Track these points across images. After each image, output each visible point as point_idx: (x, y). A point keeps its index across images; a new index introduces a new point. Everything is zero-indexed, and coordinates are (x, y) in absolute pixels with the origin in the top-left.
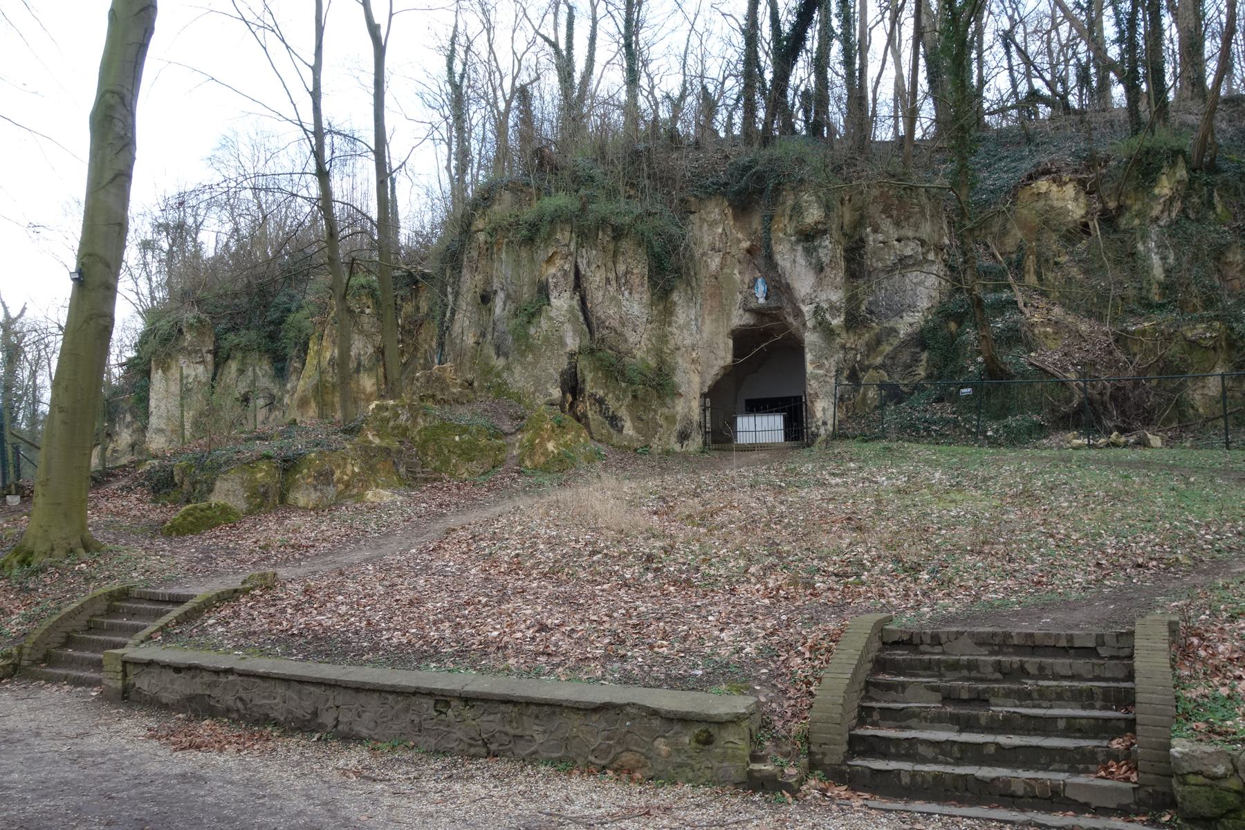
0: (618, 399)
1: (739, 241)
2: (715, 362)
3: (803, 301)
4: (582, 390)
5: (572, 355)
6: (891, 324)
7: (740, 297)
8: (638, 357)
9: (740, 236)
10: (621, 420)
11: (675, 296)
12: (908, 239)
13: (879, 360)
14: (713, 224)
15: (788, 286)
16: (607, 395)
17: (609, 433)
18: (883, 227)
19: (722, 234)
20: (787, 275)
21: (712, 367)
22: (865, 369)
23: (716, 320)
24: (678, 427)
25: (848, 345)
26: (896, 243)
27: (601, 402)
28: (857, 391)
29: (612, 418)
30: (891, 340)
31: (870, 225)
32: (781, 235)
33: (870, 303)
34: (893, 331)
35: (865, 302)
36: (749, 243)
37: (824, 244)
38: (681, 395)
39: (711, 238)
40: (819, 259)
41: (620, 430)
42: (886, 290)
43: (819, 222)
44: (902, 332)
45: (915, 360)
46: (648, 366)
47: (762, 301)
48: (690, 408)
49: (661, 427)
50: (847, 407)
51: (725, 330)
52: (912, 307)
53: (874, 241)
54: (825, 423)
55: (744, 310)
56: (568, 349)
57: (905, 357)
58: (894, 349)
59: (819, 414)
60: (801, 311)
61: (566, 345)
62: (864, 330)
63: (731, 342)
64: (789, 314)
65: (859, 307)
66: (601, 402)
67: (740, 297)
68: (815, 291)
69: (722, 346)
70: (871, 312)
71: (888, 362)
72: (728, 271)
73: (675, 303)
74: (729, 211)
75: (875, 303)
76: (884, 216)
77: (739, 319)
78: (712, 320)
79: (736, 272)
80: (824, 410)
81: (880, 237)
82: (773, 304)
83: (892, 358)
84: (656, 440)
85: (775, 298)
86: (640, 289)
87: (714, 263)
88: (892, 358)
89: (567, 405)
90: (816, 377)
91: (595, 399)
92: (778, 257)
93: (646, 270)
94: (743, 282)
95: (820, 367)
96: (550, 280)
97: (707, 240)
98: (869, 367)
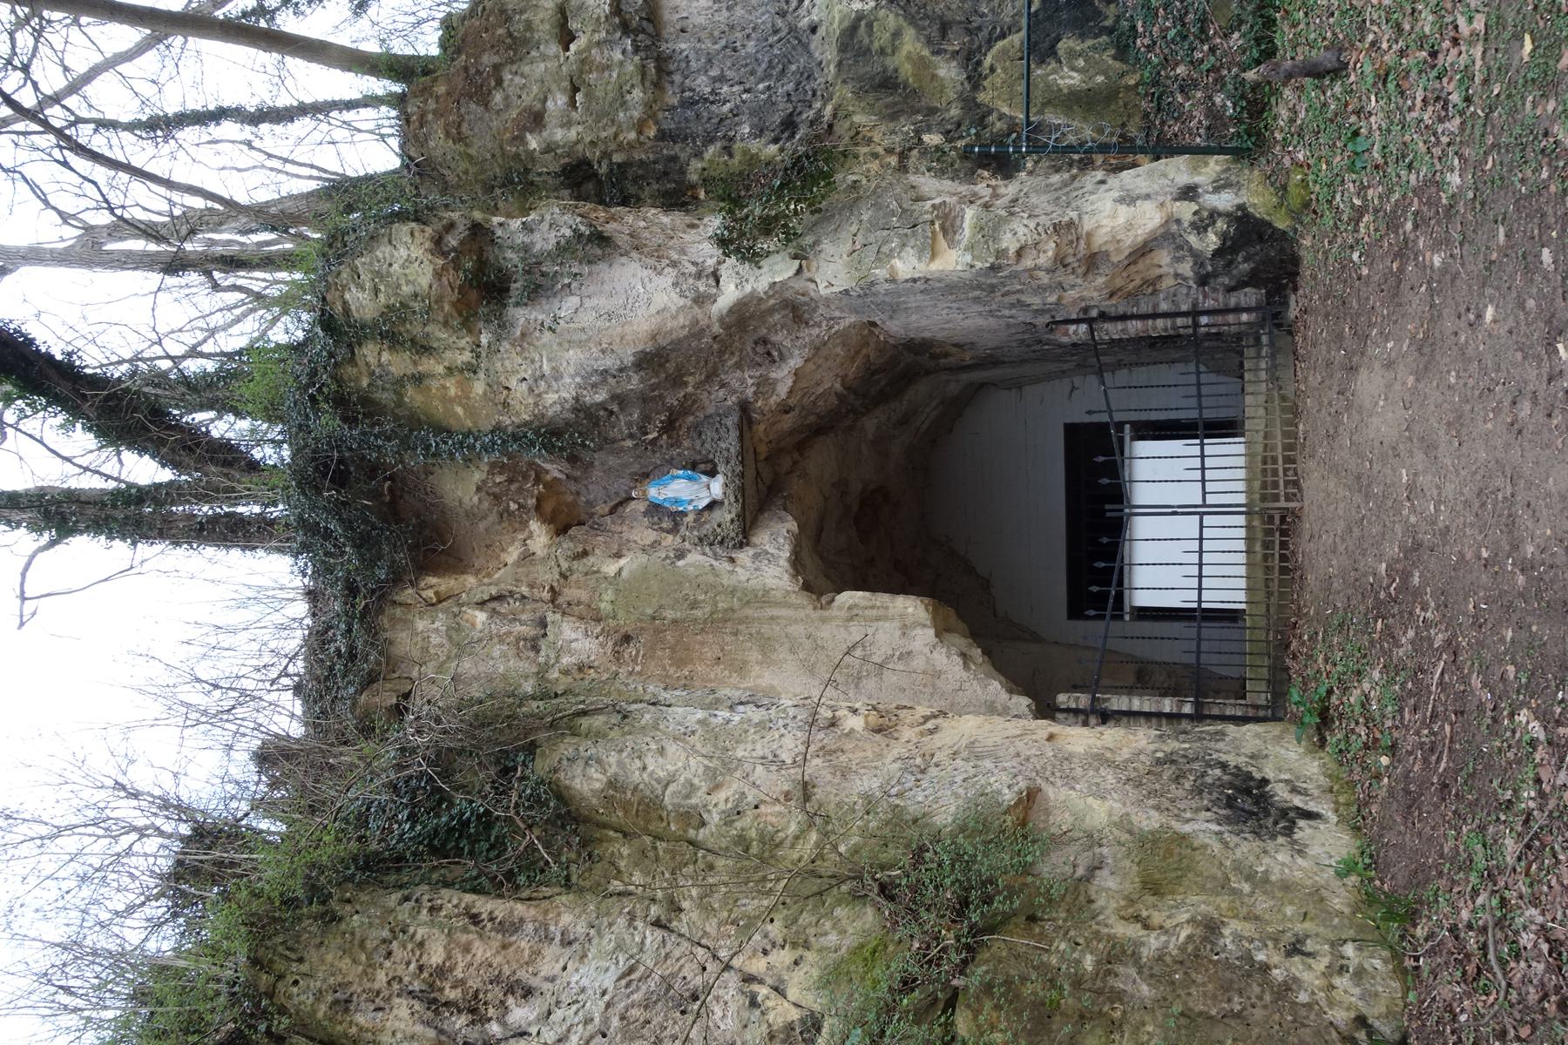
1: (527, 556)
2: (918, 663)
3: (700, 300)
8: (815, 1002)
9: (513, 554)
11: (586, 783)
13: (949, 72)
14: (461, 644)
15: (650, 360)
18: (527, 99)
20: (609, 362)
21: (938, 674)
22: (979, 115)
23: (766, 646)
24: (1203, 827)
26: (573, 47)
31: (520, 139)
32: (479, 387)
33: (759, 132)
35: (755, 145)
36: (534, 525)
37: (520, 238)
38: (1031, 797)
39: (497, 651)
40: (563, 250)
42: (721, 79)
43: (438, 241)
46: (869, 954)
47: (717, 487)
48: (1100, 760)
49: (1211, 928)
53: (567, 124)
54: (1188, 193)
55: (741, 546)
58: (912, 21)
60: (743, 317)
62: (842, 128)
63: (847, 598)
64: (765, 384)
67: (695, 557)
68: (674, 264)
70: (789, 125)
72: (609, 595)
73: (612, 784)
74: (435, 584)
75: (758, 112)
76: (498, 97)
78: (767, 661)
79: (610, 568)
80: (1129, 199)
81: (557, 102)
82: (731, 442)
83: (945, 28)
84: (1309, 974)
85: (709, 434)
88: (945, 28)
90: (988, 232)
92: (556, 399)
93: (451, 900)
95: (948, 224)
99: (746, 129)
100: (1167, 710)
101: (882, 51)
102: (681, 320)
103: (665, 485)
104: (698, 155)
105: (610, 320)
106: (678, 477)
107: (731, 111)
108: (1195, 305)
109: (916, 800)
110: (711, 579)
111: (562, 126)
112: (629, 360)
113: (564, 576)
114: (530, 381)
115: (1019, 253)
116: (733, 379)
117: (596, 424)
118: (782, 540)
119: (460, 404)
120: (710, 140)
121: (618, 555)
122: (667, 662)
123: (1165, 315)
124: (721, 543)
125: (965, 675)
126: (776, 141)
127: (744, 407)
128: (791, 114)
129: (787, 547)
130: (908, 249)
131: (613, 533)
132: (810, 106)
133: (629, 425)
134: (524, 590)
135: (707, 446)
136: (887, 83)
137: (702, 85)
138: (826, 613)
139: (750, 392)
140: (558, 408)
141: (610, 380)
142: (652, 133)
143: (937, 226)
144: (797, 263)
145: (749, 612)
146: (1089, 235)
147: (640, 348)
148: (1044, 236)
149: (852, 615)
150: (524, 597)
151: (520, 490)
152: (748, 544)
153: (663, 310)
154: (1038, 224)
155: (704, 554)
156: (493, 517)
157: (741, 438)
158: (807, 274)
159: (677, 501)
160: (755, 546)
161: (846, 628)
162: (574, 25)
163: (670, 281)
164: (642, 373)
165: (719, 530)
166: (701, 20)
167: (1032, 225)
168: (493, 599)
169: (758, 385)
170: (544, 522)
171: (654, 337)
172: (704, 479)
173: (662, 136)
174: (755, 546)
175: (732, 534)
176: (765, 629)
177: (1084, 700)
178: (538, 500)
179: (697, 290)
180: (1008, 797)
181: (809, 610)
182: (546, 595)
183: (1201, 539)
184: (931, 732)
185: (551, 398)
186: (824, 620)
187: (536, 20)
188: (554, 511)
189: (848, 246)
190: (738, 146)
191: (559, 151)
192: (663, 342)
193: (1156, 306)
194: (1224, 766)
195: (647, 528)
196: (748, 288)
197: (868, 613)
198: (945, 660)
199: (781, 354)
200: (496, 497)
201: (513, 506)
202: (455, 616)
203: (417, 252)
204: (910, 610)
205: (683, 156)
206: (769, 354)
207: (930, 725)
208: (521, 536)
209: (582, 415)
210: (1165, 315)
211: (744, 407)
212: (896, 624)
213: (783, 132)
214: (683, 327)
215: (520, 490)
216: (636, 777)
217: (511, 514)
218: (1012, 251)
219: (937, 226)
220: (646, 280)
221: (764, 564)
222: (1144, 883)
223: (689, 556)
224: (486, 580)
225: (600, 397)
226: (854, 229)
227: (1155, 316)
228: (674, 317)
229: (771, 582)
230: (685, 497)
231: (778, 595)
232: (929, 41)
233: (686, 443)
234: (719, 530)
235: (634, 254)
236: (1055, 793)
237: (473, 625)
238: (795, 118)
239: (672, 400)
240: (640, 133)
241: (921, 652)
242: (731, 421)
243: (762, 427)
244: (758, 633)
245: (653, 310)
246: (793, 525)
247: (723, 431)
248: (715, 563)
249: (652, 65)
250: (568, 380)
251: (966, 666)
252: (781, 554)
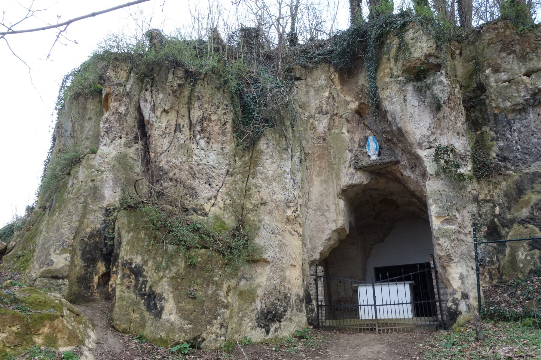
0: (158, 268)
1: (347, 103)
2: (326, 226)
3: (420, 145)
5: (108, 212)
7: (350, 155)
8: (210, 215)
9: (348, 98)
10: (162, 298)
11: (262, 145)
13: (525, 212)
14: (318, 90)
16: (145, 262)
17: (143, 318)
18: (504, 65)
19: (329, 98)
20: (398, 119)
21: (323, 232)
22: (509, 224)
23: (326, 181)
24: (259, 305)
25: (481, 197)
26: (525, 77)
27: (137, 272)
28: (502, 252)
29: (149, 295)
31: (489, 66)
32: (387, 80)
35: (495, 149)
36: (357, 103)
38: (266, 262)
39: (317, 102)
40: (434, 97)
41: (158, 314)
42: (520, 132)
43: (430, 55)
46: (223, 225)
47: (374, 157)
49: (226, 307)
50: (490, 274)
51: (335, 189)
53: (496, 82)
54: (465, 296)
55: (355, 168)
56: (105, 204)
59: (456, 284)
60: (418, 158)
61: (103, 197)
62: (500, 178)
63: (342, 203)
64: (405, 167)
66: (137, 272)
67: (350, 155)
68: (433, 133)
69: (332, 207)
70: (504, 159)
72: (337, 131)
73: (262, 152)
74: (336, 77)
75: (508, 148)
76: (504, 55)
78: (322, 182)
79: (344, 130)
80: (462, 277)
81: (504, 76)
82: (387, 159)
84: (215, 328)
86: (221, 138)
87: (322, 124)
89: (96, 279)
90: (446, 234)
91: (130, 269)
92: (387, 105)
93: (230, 117)
94: (352, 139)
95: (450, 220)
97: (314, 104)
99: (501, 144)
100: (319, 297)
101: (533, 188)
102: (413, 140)
103: (373, 141)
104: (491, 129)
105: (410, 117)
106: (376, 144)
107: (508, 138)
108: (443, 301)
109: (263, 232)
110: (342, 162)
111: (496, 80)
112: (399, 125)
113: (341, 116)
114: (390, 96)
115: (439, 244)
116: (404, 158)
117: (383, 118)
118: (359, 180)
119: (383, 74)
120: (496, 132)
121: (348, 132)
122: (319, 153)
123: (438, 291)
124: (356, 162)
125: (324, 240)
126: (498, 155)
127: (398, 162)
128: (509, 159)
129: (357, 182)
130: (439, 209)
131: (358, 128)
132: (512, 165)
133: (385, 128)
134: (336, 105)
135: (385, 152)
136: (520, 191)
137: (517, 126)
138: (336, 197)
139: (402, 163)
140: (385, 105)
141: (394, 121)
142: (496, 112)
143: (447, 217)
144: (434, 174)
145: (334, 174)
146: (450, 266)
147: (403, 128)
148: (445, 251)
149: (336, 205)
150: (334, 105)
151: (365, 97)
152: (356, 170)
153: (415, 134)
154: (449, 249)
155: (351, 158)
156: (357, 90)
157: (388, 163)
158: (431, 177)
159: (369, 145)
160: (356, 172)
161: (333, 204)
162: (533, 76)
163: (425, 134)
164: (397, 130)
165: (360, 161)
167: (448, 248)
168: (333, 96)
169: (404, 165)
170: (358, 106)
171: (406, 132)
172: (377, 153)
173: (496, 116)
174: (356, 172)
175: (358, 165)
176: (330, 180)
177: (320, 274)
178: (364, 103)
179: (423, 143)
180: (265, 256)
181: (336, 192)
182: (335, 112)
183: (368, 305)
184: (291, 233)
185: (387, 103)
186: (334, 197)
187: (534, 62)
188: (362, 108)
189: (441, 189)
190: (495, 142)
191: (487, 81)
192: (406, 135)
193: (442, 288)
194: (285, 311)
195: (360, 138)
196: (425, 159)
197: (338, 210)
198: (327, 233)
199: (414, 171)
200: (362, 90)
201: (360, 96)
202: (326, 86)
203: (425, 50)
204: (340, 222)
205: (490, 124)
206: (413, 168)
207: (293, 233)
208: (353, 100)
209: (384, 113)
210: (438, 291)
211: (398, 162)
212: (336, 218)
213: (501, 157)
214: (411, 141)
215: (365, 97)
216: (264, 158)
217: (358, 95)
218: (439, 242)
219: (447, 217)
220: (425, 126)
221: (349, 176)
222: (242, 291)
223: (350, 153)
224: (340, 92)
225: (389, 118)
226: (447, 190)
227: (438, 288)
228: (413, 137)
229: (343, 180)
230: (371, 148)
231: (339, 182)
232: (536, 204)
233: (386, 145)
234: (360, 161)
235: (435, 120)
236: (268, 268)
237: (324, 92)
238: (507, 161)
239: (395, 140)
240: (496, 108)
241: (329, 226)
242: (393, 159)
243: (394, 168)
244: (329, 178)
245: (414, 130)
246: (365, 182)
247: (390, 156)
248: (348, 162)
249: (521, 107)
250: (392, 107)
251: (326, 240)
252: (354, 181)
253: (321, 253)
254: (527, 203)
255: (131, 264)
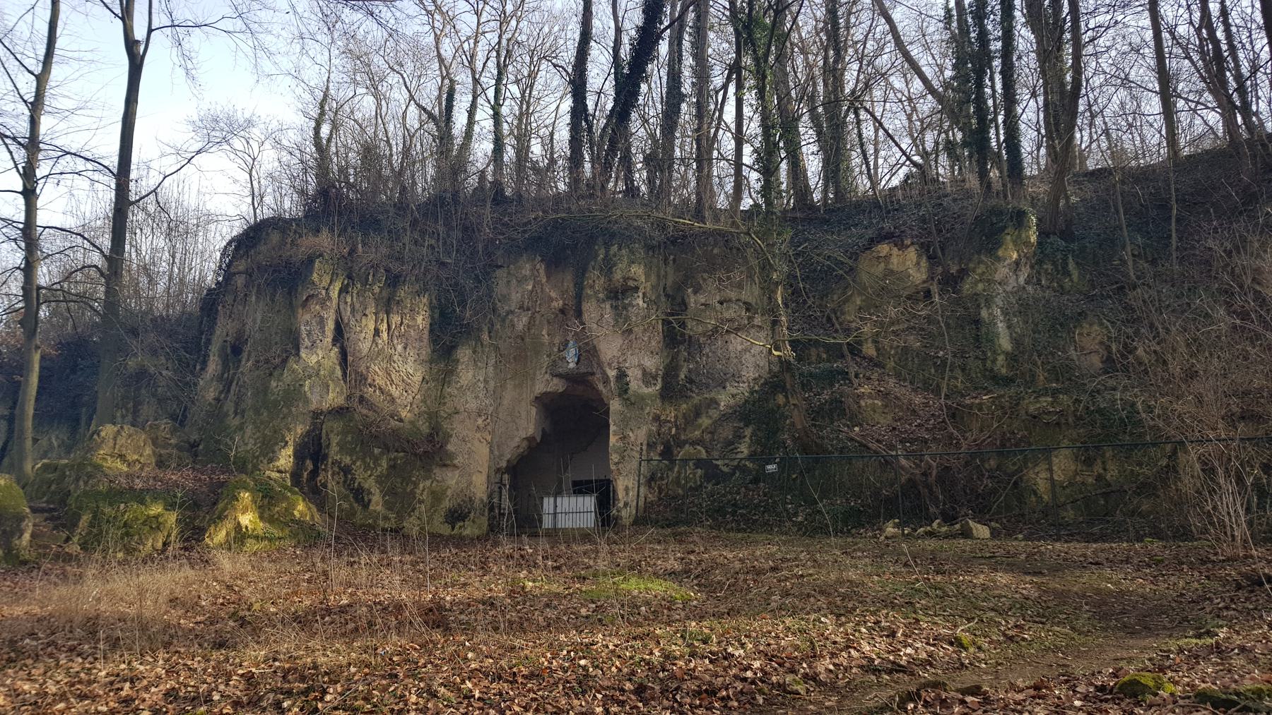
0: (367, 468)
1: (551, 299)
2: (516, 433)
4: (326, 457)
6: (713, 395)
10: (370, 493)
12: (730, 300)
16: (354, 463)
17: (352, 507)
19: (532, 291)
22: (681, 444)
25: (663, 418)
27: (346, 470)
28: (671, 469)
30: (711, 412)
33: (690, 371)
34: (714, 403)
41: (366, 506)
44: (722, 404)
45: (739, 437)
47: (572, 365)
50: (660, 488)
51: (528, 396)
52: (737, 377)
53: (696, 302)
57: (727, 432)
59: (621, 494)
63: (534, 411)
65: (678, 376)
66: (346, 470)
69: (524, 414)
70: (691, 381)
71: (707, 437)
74: (541, 268)
77: (545, 383)
78: (515, 386)
80: (627, 489)
82: (583, 370)
86: (417, 345)
87: (521, 322)
88: (711, 433)
91: (340, 467)
96: (303, 328)
97: (515, 297)
98: (685, 442)
109: (453, 440)
120: (689, 354)
136: (698, 415)
149: (528, 413)
166: (731, 348)
173: (690, 337)
180: (456, 462)
194: (470, 513)
216: (460, 367)
236: (457, 472)
242: (590, 370)
246: (561, 390)
253: (508, 461)
254: (700, 426)
255: (340, 463)
